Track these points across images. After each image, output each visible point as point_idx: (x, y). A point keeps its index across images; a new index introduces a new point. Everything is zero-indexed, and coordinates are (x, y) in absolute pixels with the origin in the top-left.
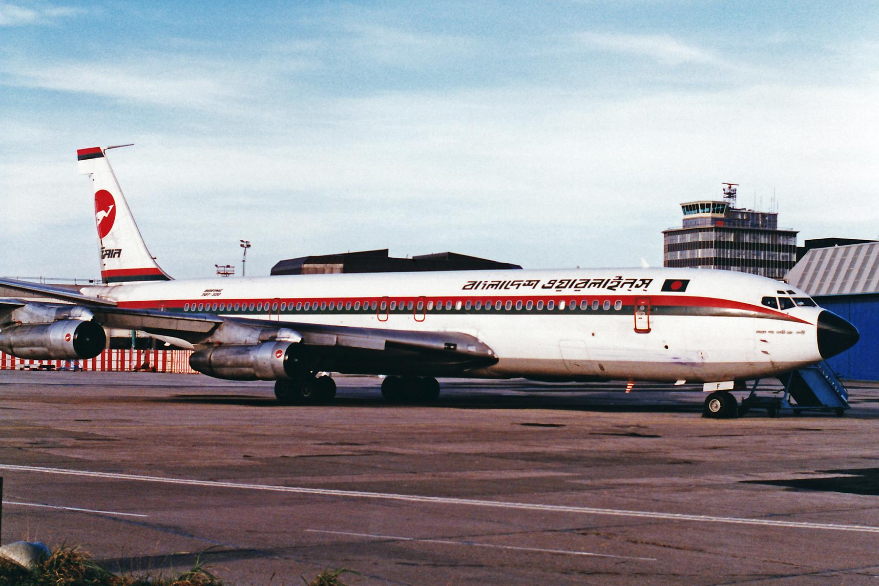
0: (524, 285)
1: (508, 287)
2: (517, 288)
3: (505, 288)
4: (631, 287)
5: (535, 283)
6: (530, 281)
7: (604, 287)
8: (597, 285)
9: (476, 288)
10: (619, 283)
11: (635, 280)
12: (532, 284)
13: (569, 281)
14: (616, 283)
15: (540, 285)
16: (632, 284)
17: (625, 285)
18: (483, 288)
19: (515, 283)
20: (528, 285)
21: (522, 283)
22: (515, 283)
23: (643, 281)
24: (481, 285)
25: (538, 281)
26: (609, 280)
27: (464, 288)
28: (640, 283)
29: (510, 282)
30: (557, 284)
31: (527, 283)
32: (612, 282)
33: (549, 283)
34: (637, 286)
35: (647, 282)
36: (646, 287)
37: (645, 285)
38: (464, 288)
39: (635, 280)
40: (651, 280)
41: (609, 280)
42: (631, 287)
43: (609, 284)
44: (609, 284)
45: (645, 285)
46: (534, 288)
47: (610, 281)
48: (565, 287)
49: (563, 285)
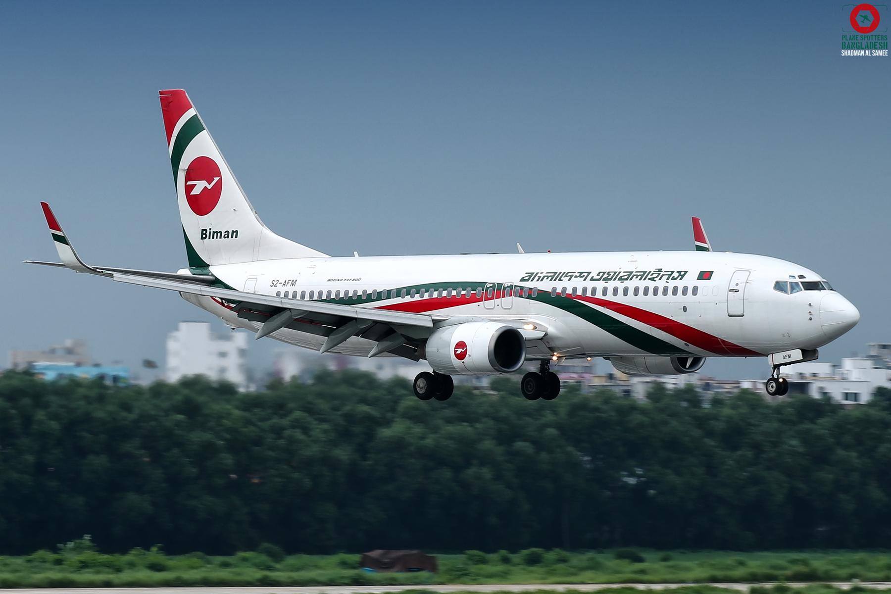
0: (575, 277)
2: (569, 280)
3: (560, 280)
5: (586, 274)
6: (581, 273)
13: (616, 272)
16: (670, 276)
17: (664, 276)
18: (538, 280)
20: (580, 276)
21: (575, 274)
23: (679, 272)
27: (522, 280)
28: (676, 275)
30: (606, 275)
31: (578, 275)
33: (598, 275)
35: (682, 273)
37: (680, 277)
38: (522, 280)
43: (649, 277)
44: (649, 277)
46: (585, 280)
47: (651, 273)
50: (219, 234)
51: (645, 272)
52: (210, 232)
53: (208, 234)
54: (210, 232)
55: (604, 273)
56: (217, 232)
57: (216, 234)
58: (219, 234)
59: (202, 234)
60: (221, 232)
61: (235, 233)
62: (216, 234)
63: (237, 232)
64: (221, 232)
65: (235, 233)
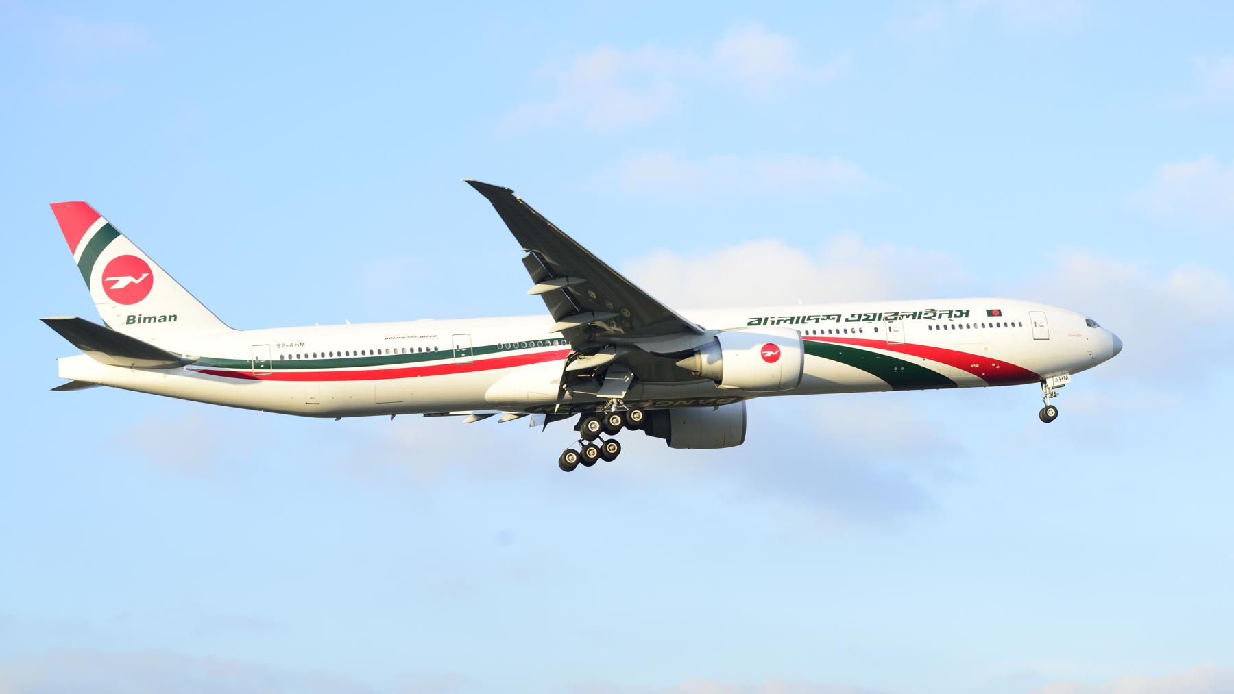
0: (822, 319)
1: (806, 321)
3: (803, 322)
4: (950, 316)
5: (836, 317)
7: (919, 318)
8: (911, 317)
9: (765, 323)
10: (935, 315)
11: (951, 312)
12: (833, 319)
14: (932, 315)
15: (843, 319)
18: (773, 322)
19: (811, 318)
22: (811, 318)
23: (961, 311)
24: (769, 322)
25: (839, 316)
26: (921, 313)
27: (750, 324)
28: (958, 314)
29: (804, 317)
30: (863, 317)
31: (825, 317)
32: (926, 314)
33: (853, 316)
34: (956, 316)
35: (965, 312)
36: (967, 316)
37: (964, 315)
38: (750, 324)
39: (951, 312)
40: (968, 311)
41: (921, 313)
42: (950, 316)
43: (923, 316)
45: (964, 315)
47: (923, 314)
48: (874, 319)
49: (871, 318)
50: (152, 319)
51: (915, 313)
52: (140, 319)
53: (137, 319)
54: (140, 319)
55: (860, 316)
56: (150, 318)
57: (147, 320)
58: (152, 319)
59: (129, 317)
60: (155, 318)
61: (173, 318)
62: (147, 320)
63: (175, 317)
64: (155, 318)
65: (173, 318)
